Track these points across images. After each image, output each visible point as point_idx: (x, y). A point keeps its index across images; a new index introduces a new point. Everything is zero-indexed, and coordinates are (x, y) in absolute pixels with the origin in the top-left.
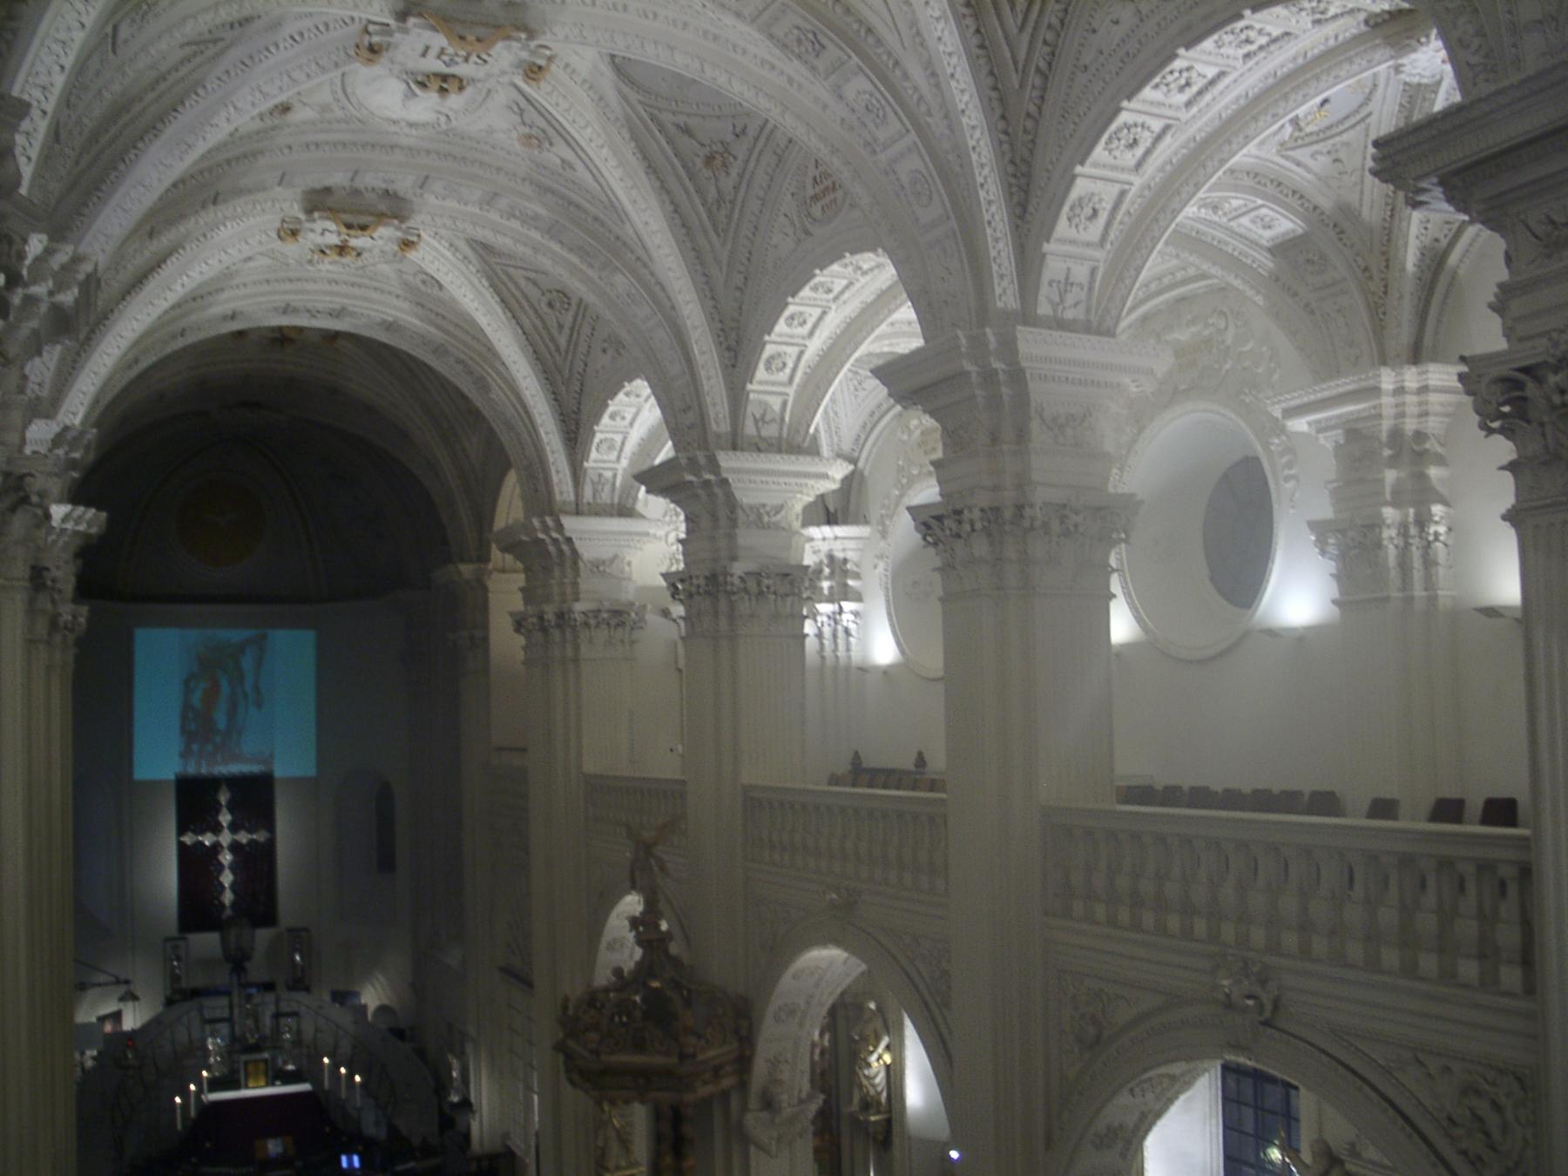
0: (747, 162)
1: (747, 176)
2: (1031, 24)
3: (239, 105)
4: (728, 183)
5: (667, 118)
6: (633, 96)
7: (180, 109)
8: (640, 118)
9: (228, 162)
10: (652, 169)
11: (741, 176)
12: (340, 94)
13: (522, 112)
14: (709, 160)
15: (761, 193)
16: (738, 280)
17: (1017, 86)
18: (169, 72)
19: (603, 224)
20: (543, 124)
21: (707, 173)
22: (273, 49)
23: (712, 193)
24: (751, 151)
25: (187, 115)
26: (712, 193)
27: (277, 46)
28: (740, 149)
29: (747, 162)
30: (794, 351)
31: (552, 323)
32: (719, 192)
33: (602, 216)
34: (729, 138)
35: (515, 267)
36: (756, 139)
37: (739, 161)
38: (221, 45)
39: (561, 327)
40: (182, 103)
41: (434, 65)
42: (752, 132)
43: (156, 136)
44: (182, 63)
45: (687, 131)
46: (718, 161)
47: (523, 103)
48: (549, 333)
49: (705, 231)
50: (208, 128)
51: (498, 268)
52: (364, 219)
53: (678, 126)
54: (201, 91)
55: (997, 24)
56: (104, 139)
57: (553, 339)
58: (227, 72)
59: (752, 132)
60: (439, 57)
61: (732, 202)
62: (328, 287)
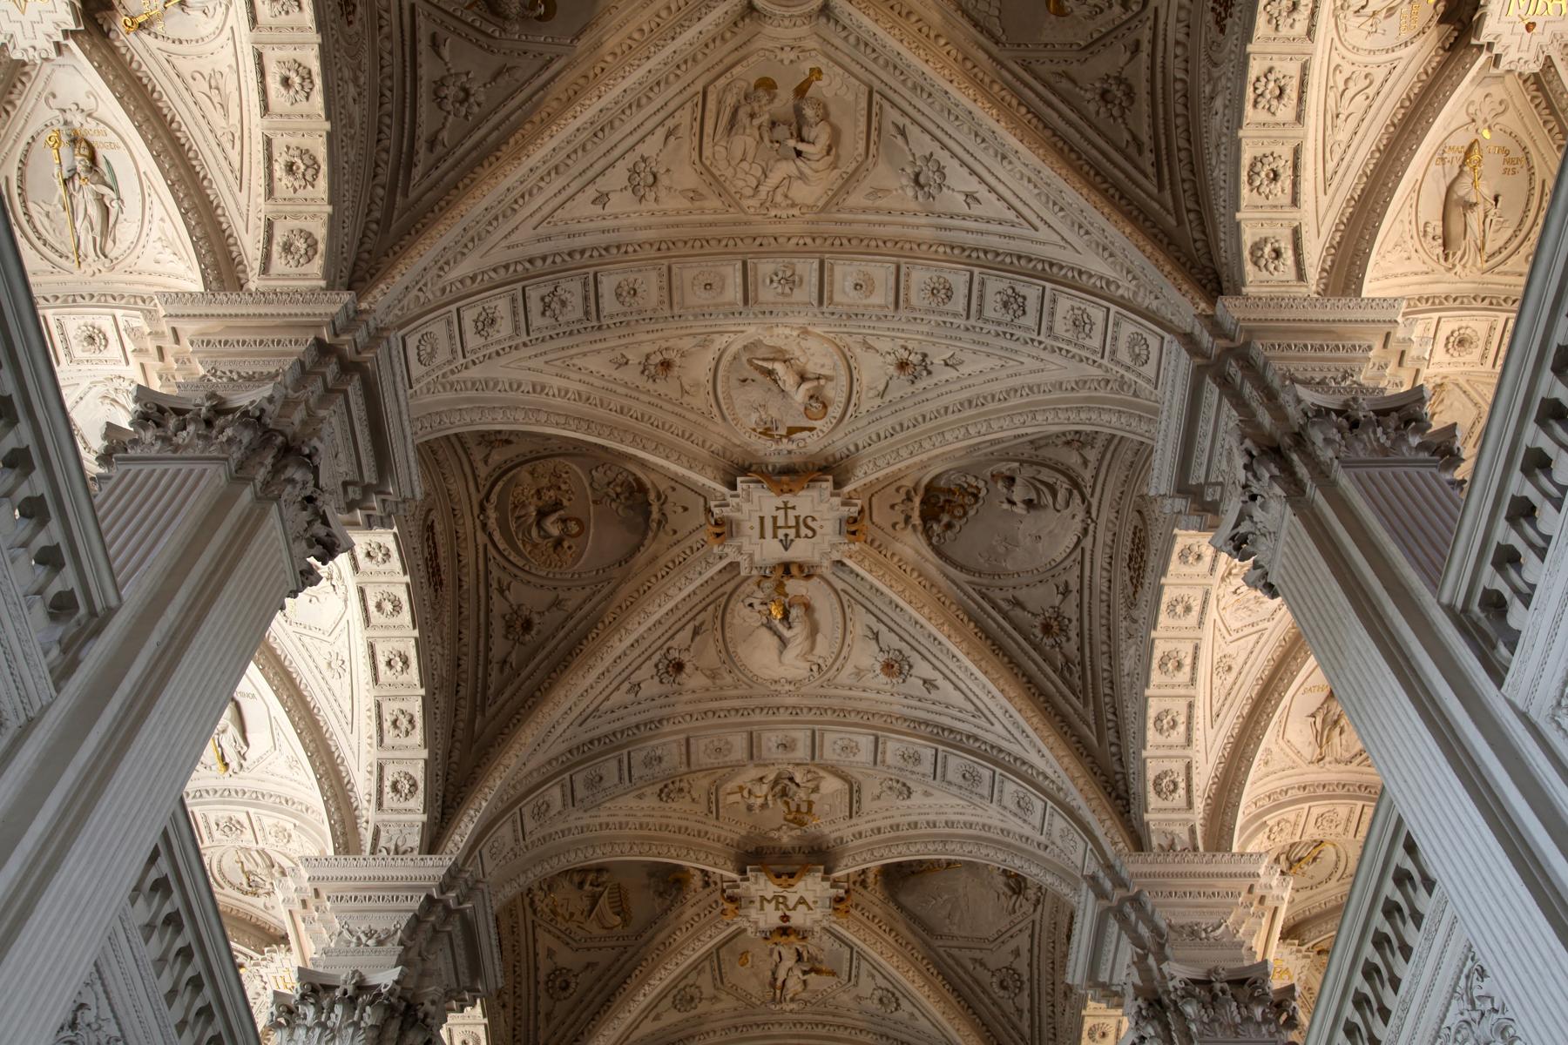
0: (1080, 620)
1: (1087, 636)
2: (1167, 183)
4: (1071, 647)
5: (997, 595)
6: (961, 577)
7: (585, 642)
8: (974, 600)
9: (637, 727)
10: (998, 648)
11: (1080, 635)
12: (723, 655)
13: (876, 636)
14: (1047, 628)
15: (1105, 648)
16: (1111, 736)
17: (1174, 223)
18: (575, 611)
19: (976, 739)
20: (896, 643)
21: (1050, 641)
23: (1059, 660)
24: (1080, 606)
26: (1059, 660)
27: (656, 576)
28: (1070, 610)
29: (1080, 620)
30: (1178, 767)
31: (1009, 1007)
32: (1064, 655)
33: (975, 731)
34: (1057, 600)
35: (960, 948)
36: (1080, 591)
37: (1075, 622)
38: (614, 583)
39: (1019, 1011)
40: (586, 638)
41: (771, 551)
42: (1074, 586)
43: (566, 667)
44: (584, 602)
45: (1017, 603)
46: (1056, 629)
47: (877, 626)
48: (1009, 1020)
49: (1064, 697)
51: (941, 951)
52: (790, 869)
53: (1009, 601)
54: (600, 626)
55: (1138, 191)
56: (524, 674)
57: (1014, 1027)
58: (620, 607)
59: (1074, 586)
60: (775, 536)
61: (1082, 663)
62: (794, 1031)
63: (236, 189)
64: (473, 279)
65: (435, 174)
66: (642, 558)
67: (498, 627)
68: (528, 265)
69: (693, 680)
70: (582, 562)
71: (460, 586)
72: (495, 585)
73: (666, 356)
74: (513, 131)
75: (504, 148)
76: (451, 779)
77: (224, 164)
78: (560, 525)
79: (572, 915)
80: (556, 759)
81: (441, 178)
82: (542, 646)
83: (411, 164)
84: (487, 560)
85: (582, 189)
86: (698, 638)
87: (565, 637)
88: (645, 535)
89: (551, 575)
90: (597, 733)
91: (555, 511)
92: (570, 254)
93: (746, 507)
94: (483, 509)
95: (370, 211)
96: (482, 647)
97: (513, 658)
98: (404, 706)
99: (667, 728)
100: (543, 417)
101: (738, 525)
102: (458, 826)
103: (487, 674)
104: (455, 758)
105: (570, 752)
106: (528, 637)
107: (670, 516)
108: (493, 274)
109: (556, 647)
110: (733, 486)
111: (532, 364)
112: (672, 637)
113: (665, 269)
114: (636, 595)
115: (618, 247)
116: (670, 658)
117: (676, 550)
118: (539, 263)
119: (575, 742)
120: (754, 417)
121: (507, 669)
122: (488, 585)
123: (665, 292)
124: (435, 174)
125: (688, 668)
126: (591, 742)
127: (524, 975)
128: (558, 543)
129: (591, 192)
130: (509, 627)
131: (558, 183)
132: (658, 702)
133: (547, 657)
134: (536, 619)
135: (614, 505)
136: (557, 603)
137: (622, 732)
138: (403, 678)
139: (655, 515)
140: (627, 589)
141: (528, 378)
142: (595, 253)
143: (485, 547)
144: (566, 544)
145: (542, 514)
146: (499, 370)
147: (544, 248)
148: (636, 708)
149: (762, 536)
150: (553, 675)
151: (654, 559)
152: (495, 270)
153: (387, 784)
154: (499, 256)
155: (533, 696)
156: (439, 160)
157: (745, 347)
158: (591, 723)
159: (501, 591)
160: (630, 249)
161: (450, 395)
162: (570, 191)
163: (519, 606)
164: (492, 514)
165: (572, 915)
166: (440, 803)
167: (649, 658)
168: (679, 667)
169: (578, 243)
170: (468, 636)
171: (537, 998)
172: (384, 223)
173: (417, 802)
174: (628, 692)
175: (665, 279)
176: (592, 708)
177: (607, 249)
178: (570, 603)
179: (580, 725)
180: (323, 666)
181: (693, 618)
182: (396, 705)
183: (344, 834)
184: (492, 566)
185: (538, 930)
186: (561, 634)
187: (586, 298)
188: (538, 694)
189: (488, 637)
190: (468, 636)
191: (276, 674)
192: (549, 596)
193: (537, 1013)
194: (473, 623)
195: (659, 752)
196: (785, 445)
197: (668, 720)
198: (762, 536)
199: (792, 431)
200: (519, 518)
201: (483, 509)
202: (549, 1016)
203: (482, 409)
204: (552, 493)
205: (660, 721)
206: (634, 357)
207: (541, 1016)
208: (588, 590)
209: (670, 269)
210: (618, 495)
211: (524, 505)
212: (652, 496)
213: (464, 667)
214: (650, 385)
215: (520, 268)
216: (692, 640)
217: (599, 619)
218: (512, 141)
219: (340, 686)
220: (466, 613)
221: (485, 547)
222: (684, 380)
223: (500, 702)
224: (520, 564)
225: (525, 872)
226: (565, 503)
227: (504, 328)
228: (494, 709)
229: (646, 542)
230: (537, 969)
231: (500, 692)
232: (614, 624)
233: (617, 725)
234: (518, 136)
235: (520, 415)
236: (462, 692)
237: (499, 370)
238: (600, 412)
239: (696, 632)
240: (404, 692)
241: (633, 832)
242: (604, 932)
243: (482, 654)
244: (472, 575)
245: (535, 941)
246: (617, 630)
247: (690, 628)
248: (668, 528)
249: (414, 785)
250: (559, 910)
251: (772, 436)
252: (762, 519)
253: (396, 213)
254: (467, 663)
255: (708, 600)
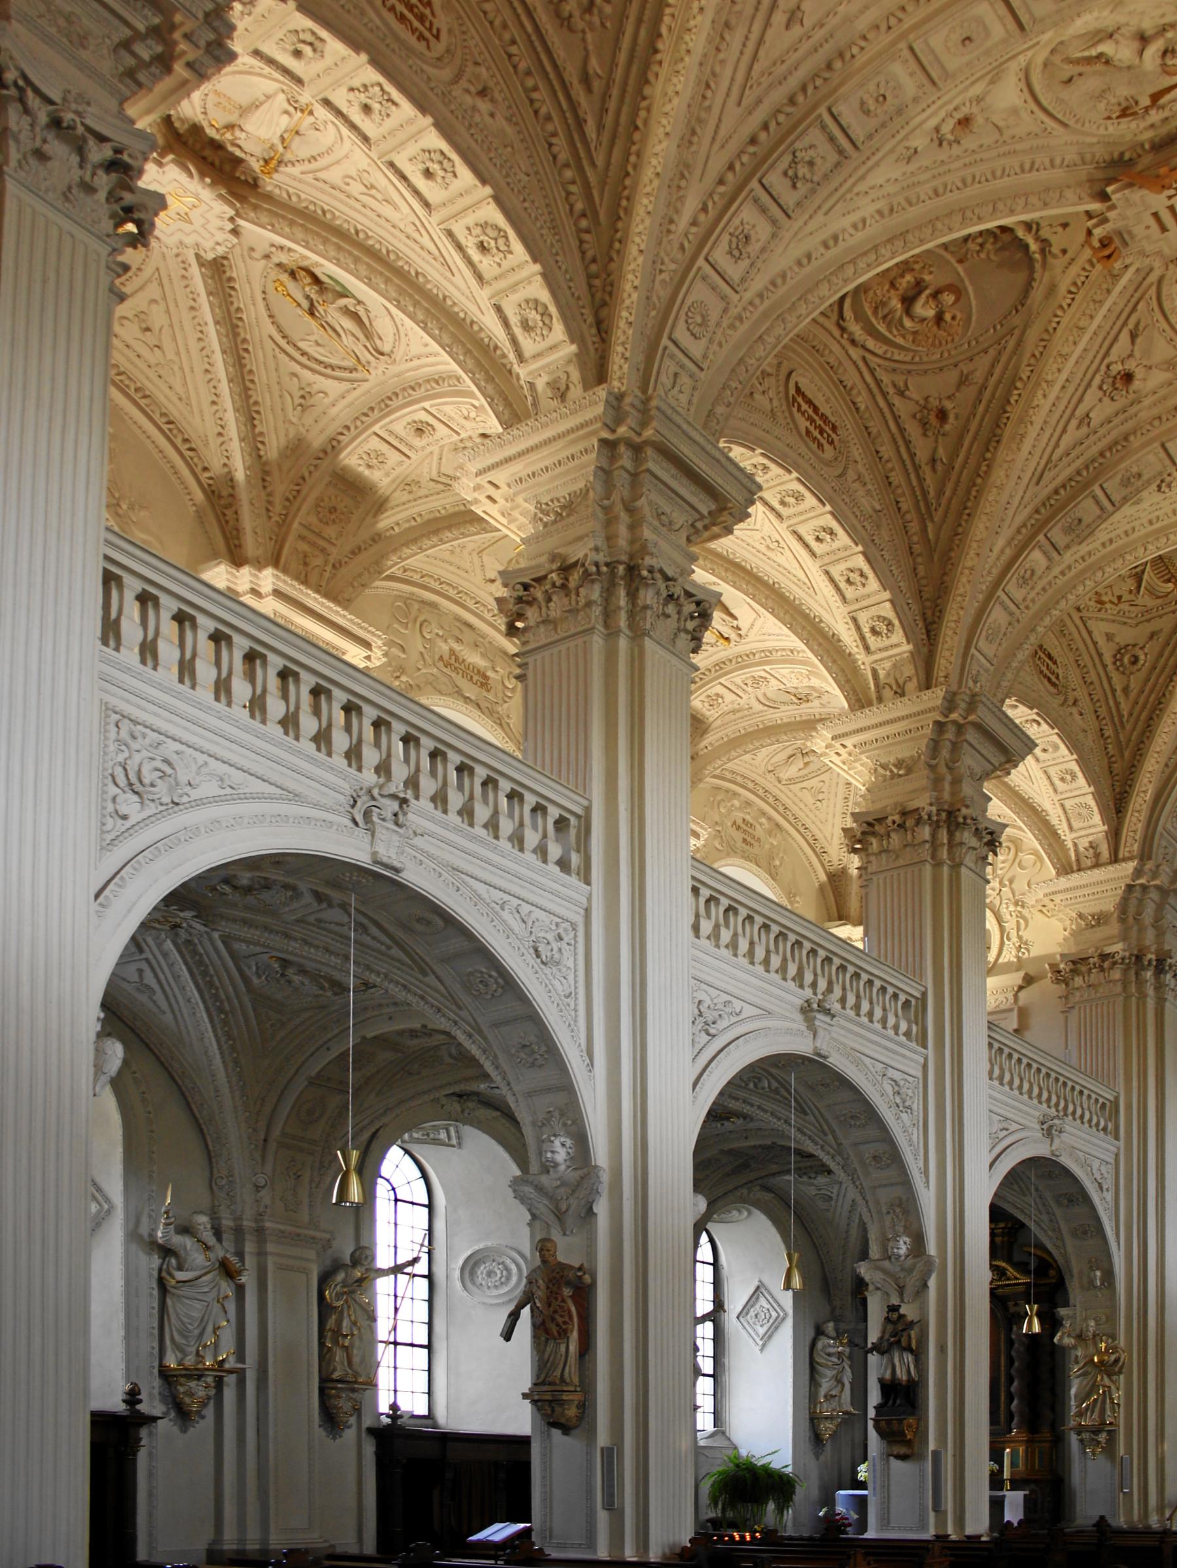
3: (1049, 378)
7: (1008, 408)
9: (1102, 454)
18: (987, 380)
22: (1059, 313)
25: (1014, 412)
27: (1061, 307)
38: (1016, 332)
40: (1009, 402)
44: (993, 366)
50: (1031, 412)
54: (1019, 384)
56: (957, 465)
58: (1034, 355)
63: (449, 274)
64: (705, 209)
65: (609, 120)
66: (1037, 293)
67: (913, 430)
68: (752, 149)
69: (1149, 382)
70: (973, 324)
71: (857, 409)
72: (891, 390)
73: (958, 116)
74: (658, 19)
75: (660, 46)
76: (925, 596)
77: (425, 254)
78: (932, 304)
79: (1120, 598)
80: (1024, 525)
81: (617, 123)
82: (965, 429)
83: (580, 123)
84: (872, 372)
85: (767, 24)
86: (1139, 340)
87: (986, 411)
88: (1032, 270)
89: (946, 355)
90: (1058, 481)
91: (920, 293)
92: (792, 101)
93: (1130, 213)
94: (843, 329)
95: (572, 207)
96: (905, 456)
97: (941, 453)
98: (850, 564)
99: (1135, 442)
100: (850, 270)
101: (1129, 232)
102: (945, 642)
103: (921, 480)
104: (921, 573)
105: (1037, 511)
106: (947, 427)
107: (1053, 239)
108: (722, 189)
109: (980, 425)
110: (1104, 197)
111: (812, 226)
112: (1107, 354)
113: (906, 53)
114: (1046, 337)
115: (841, 55)
116: (1114, 373)
117: (1074, 269)
118: (763, 136)
119: (1037, 501)
120: (1102, 106)
121: (939, 467)
122: (884, 395)
123: (920, 74)
124: (609, 120)
125: (1139, 373)
126: (1056, 492)
127: (1090, 665)
128: (939, 318)
129: (779, 18)
130: (924, 424)
131: (735, 39)
132: (1116, 421)
133: (975, 438)
134: (948, 405)
135: (983, 255)
136: (963, 381)
137: (1087, 467)
138: (837, 544)
139: (1034, 247)
140: (1033, 335)
141: (812, 243)
142: (818, 82)
143: (864, 358)
144: (948, 317)
145: (908, 301)
146: (782, 259)
147: (759, 116)
148: (1093, 438)
149: (1164, 229)
150: (988, 455)
151: (1052, 289)
152: (721, 182)
153: (866, 630)
154: (717, 165)
155: (974, 485)
156: (603, 101)
157: (1053, 51)
158: (1048, 475)
159: (901, 394)
160: (855, 50)
161: (742, 328)
162: (754, 37)
163: (926, 399)
164: (856, 329)
165: (1120, 598)
166: (921, 624)
167: (1089, 385)
168: (1128, 377)
169: (793, 82)
170: (887, 451)
171: (1109, 679)
172: (590, 212)
173: (898, 636)
174: (1078, 427)
175: (912, 60)
176: (1043, 463)
177: (829, 67)
178: (978, 374)
179: (1038, 483)
180: (763, 549)
181: (1125, 324)
182: (842, 566)
183: (848, 681)
184: (880, 373)
185: (1089, 623)
186: (981, 408)
187: (832, 139)
188: (979, 481)
189: (908, 443)
190: (887, 451)
191: (727, 570)
192: (953, 376)
193: (1113, 691)
194: (885, 437)
195: (1135, 470)
196: (1155, 116)
197: (1135, 433)
198: (1164, 229)
199: (1155, 97)
200: (885, 317)
201: (843, 329)
202: (1126, 690)
203: (781, 318)
204: (909, 278)
205: (1126, 439)
206: (919, 141)
207: (1119, 693)
208: (992, 352)
209: (912, 49)
210: (981, 245)
211: (883, 304)
212: (1020, 233)
213: (895, 483)
214: (956, 150)
215: (745, 158)
216: (1133, 342)
217: (1015, 377)
218: (664, 30)
219: (787, 560)
220: (874, 431)
221: (864, 358)
222: (996, 119)
223: (944, 501)
224: (908, 358)
225: (1033, 630)
226: (927, 277)
227: (762, 231)
228: (941, 510)
229: (1036, 276)
230: (1100, 655)
231: (940, 492)
232: (1034, 379)
233: (1078, 463)
234: (667, 19)
235: (824, 290)
236: (904, 506)
237: (782, 259)
238: (913, 212)
239: (1133, 336)
240: (842, 554)
241: (1143, 531)
242: (1159, 601)
243: (908, 462)
244: (864, 392)
245: (1090, 633)
246: (1038, 384)
247: (1125, 337)
248: (1055, 250)
249: (890, 624)
250: (1105, 598)
251: (1135, 114)
252: (1155, 215)
253: (595, 193)
254: (897, 477)
255: (1133, 300)
